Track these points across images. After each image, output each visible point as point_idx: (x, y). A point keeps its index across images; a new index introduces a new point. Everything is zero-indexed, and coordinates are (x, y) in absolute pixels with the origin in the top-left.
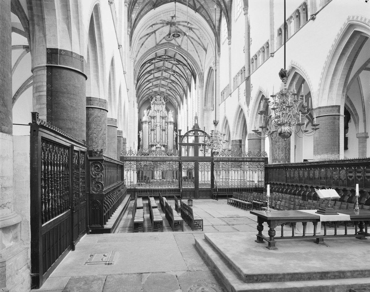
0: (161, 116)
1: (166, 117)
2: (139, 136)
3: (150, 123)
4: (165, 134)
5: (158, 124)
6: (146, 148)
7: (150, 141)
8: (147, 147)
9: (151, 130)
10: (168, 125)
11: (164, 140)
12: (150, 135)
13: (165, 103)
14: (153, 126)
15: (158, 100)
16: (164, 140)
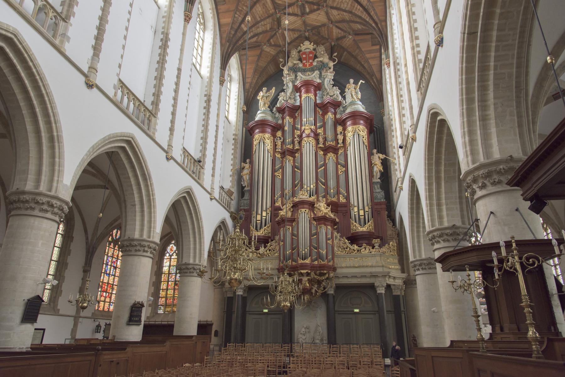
0: (316, 105)
1: (336, 105)
2: (240, 178)
3: (279, 134)
4: (337, 163)
5: (307, 129)
6: (259, 217)
7: (278, 193)
8: (268, 211)
9: (283, 154)
10: (345, 129)
11: (332, 183)
12: (278, 174)
13: (331, 64)
14: (288, 140)
15: (305, 59)
16: (332, 183)
